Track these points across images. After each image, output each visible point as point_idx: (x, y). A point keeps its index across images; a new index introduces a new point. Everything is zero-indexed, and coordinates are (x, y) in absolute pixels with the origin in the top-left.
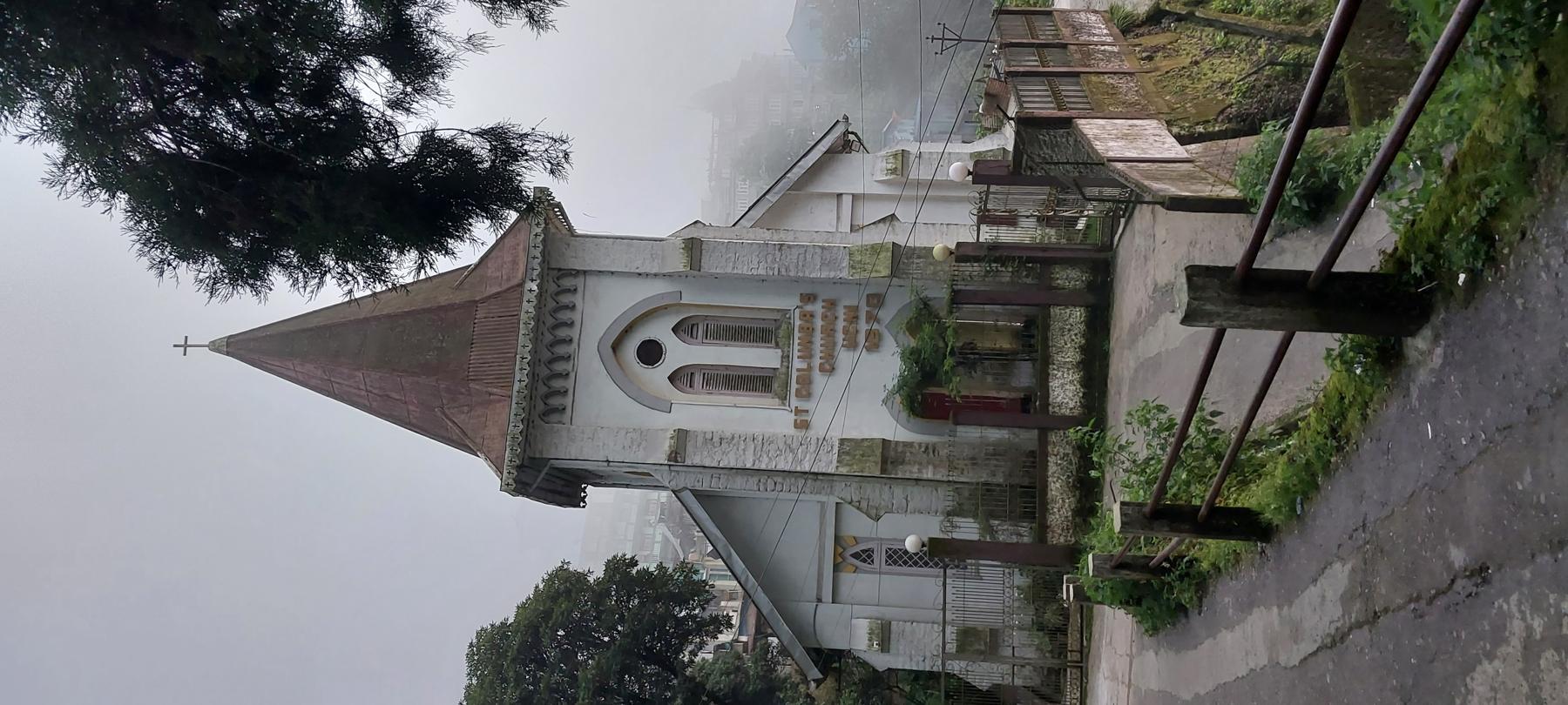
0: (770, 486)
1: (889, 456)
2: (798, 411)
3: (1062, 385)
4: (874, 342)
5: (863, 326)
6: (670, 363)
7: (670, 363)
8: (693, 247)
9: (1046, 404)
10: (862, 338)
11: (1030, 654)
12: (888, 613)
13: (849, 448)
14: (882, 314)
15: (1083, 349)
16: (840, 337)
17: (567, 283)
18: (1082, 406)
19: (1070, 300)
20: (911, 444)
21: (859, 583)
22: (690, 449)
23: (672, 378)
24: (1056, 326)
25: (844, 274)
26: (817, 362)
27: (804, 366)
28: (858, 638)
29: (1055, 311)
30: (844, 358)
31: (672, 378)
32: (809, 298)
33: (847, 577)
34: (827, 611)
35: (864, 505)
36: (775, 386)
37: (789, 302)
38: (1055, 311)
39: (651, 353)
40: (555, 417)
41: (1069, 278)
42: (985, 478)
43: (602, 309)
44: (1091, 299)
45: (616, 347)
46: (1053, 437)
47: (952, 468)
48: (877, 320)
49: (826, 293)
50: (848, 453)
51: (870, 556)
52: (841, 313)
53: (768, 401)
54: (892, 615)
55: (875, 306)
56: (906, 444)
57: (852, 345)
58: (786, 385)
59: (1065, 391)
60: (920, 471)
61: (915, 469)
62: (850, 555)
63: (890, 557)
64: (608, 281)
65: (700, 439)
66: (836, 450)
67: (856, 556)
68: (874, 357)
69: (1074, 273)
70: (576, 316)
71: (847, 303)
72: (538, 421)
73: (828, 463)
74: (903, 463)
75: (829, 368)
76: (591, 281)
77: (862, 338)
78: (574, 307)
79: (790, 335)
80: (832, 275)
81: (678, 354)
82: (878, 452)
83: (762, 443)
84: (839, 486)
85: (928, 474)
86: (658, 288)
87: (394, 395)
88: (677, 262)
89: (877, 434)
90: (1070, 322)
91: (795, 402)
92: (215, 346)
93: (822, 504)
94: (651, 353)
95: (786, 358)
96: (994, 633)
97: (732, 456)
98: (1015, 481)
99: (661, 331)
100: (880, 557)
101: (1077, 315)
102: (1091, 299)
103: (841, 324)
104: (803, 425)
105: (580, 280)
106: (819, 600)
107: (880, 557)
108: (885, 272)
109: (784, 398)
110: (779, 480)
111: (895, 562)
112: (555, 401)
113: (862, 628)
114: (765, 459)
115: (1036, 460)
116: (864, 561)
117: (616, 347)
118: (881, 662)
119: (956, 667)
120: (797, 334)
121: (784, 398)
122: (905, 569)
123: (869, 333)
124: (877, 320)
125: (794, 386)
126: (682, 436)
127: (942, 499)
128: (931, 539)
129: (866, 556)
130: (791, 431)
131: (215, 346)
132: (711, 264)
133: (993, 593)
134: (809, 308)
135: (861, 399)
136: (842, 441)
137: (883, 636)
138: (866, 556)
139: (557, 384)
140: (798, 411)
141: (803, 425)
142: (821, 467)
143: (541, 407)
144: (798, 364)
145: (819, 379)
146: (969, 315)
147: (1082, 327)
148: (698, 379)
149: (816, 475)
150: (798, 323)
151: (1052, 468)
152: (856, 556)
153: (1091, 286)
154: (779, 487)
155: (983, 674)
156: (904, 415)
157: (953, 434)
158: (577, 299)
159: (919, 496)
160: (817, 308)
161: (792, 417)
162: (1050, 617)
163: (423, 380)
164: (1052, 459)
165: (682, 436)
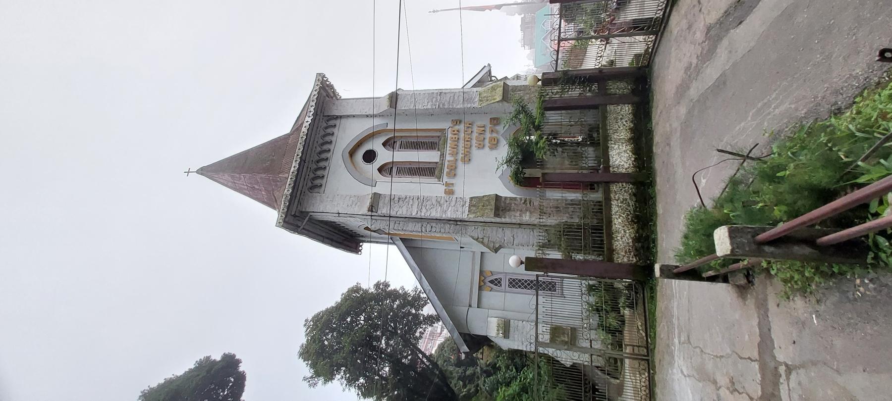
0: (429, 229)
1: (500, 206)
2: (447, 184)
3: (619, 154)
4: (495, 145)
5: (488, 135)
6: (379, 162)
7: (379, 162)
8: (394, 98)
9: (607, 167)
10: (487, 141)
11: (597, 345)
12: (509, 315)
13: (476, 203)
14: (497, 128)
15: (632, 130)
16: (474, 142)
17: (332, 123)
18: (635, 167)
19: (621, 100)
20: (515, 199)
21: (493, 297)
22: (381, 204)
23: (380, 170)
24: (611, 117)
25: (476, 105)
26: (460, 156)
27: (452, 159)
28: (492, 331)
29: (611, 108)
30: (475, 152)
31: (380, 170)
32: (457, 122)
33: (486, 294)
34: (474, 313)
35: (486, 240)
36: (436, 172)
37: (445, 125)
38: (611, 108)
39: (370, 156)
40: (316, 190)
41: (618, 88)
42: (565, 218)
43: (347, 135)
44: (636, 99)
45: (352, 153)
46: (614, 188)
47: (542, 213)
48: (497, 132)
49: (468, 119)
50: (474, 206)
51: (499, 282)
52: (475, 129)
53: (433, 180)
54: (515, 319)
55: (495, 125)
56: (511, 199)
57: (481, 147)
58: (441, 170)
59: (621, 157)
60: (521, 216)
61: (518, 214)
62: (488, 281)
63: (511, 283)
64: (351, 120)
65: (388, 199)
66: (467, 205)
67: (492, 282)
68: (494, 153)
69: (622, 85)
70: (333, 139)
71: (479, 123)
72: (307, 192)
73: (463, 213)
74: (509, 210)
75: (467, 159)
76: (343, 121)
77: (487, 141)
78: (333, 134)
79: (445, 141)
80: (469, 106)
81: (384, 156)
82: (493, 203)
83: (422, 201)
84: (471, 229)
85: (526, 218)
86: (378, 122)
87: (256, 187)
88: (385, 106)
89: (493, 192)
90: (621, 119)
91: (445, 179)
92: (197, 172)
93: (474, 252)
94: (370, 156)
95: (442, 156)
96: (574, 330)
97: (404, 209)
98: (588, 221)
99: (376, 145)
100: (505, 283)
101: (626, 110)
102: (636, 99)
103: (475, 135)
104: (450, 192)
105: (337, 122)
106: (470, 306)
107: (505, 283)
108: (499, 98)
109: (439, 178)
110: (434, 225)
111: (514, 286)
112: (318, 182)
113: (494, 323)
114: (424, 210)
115: (602, 210)
116: (496, 285)
117: (352, 153)
118: (506, 344)
119: (550, 351)
120: (449, 141)
121: (439, 178)
122: (519, 290)
123: (491, 139)
124: (497, 132)
125: (446, 170)
126: (376, 197)
127: (535, 237)
128: (527, 258)
129: (497, 282)
130: (443, 195)
131: (197, 172)
132: (402, 105)
133: (572, 300)
134: (457, 127)
135: (486, 173)
136: (471, 198)
137: (506, 329)
138: (497, 282)
139: (319, 173)
140: (447, 184)
141: (450, 192)
142: (459, 216)
143: (310, 184)
144: (448, 158)
145: (460, 165)
146: (553, 117)
147: (631, 116)
148: (395, 170)
149: (456, 221)
150: (450, 135)
151: (615, 209)
152: (492, 282)
153: (634, 92)
154: (434, 230)
155: (567, 357)
156: (512, 183)
157: (542, 197)
158: (335, 130)
159: (522, 235)
160: (461, 127)
161: (444, 187)
162: (613, 322)
163: (263, 175)
164: (614, 203)
165: (376, 197)
